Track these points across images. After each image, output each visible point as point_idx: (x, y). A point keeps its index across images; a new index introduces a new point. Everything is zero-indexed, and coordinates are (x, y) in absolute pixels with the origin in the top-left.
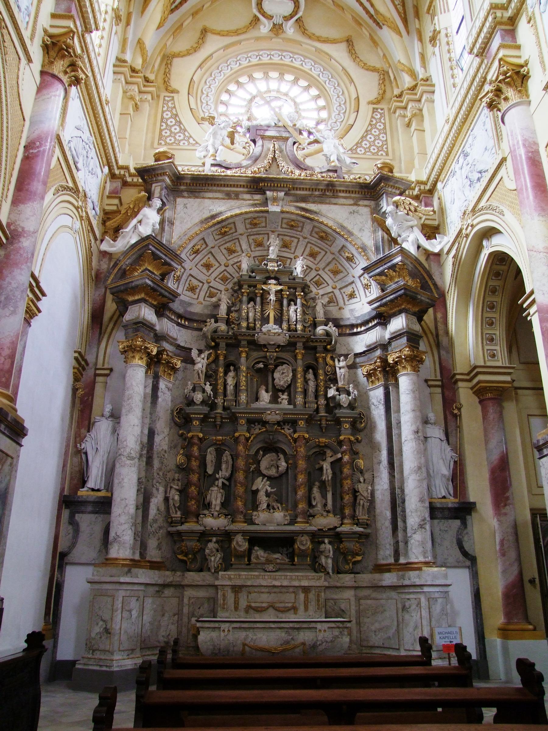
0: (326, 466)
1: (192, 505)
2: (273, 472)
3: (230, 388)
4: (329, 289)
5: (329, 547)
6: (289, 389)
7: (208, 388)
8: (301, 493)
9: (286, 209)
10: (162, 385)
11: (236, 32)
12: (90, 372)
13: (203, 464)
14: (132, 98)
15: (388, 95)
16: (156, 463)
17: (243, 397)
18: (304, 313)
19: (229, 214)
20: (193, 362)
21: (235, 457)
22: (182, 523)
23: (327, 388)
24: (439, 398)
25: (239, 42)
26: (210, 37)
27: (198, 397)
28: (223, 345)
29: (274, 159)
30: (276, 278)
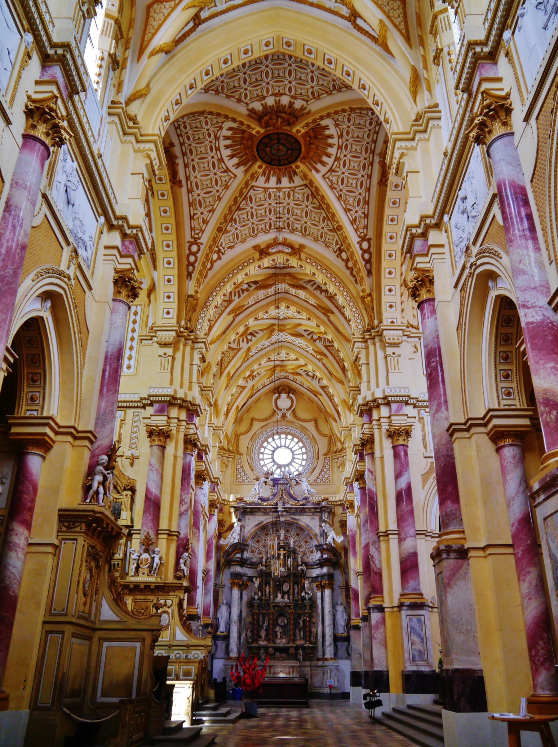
0: (301, 622)
1: (255, 636)
2: (282, 624)
3: (267, 592)
4: (304, 549)
5: (301, 652)
6: (288, 593)
7: (260, 594)
8: (291, 632)
9: (287, 519)
10: (244, 593)
11: (266, 419)
12: (217, 587)
13: (258, 621)
14: (225, 463)
15: (332, 449)
16: (243, 622)
17: (272, 597)
18: (293, 562)
19: (265, 522)
20: (253, 582)
21: (269, 619)
22: (252, 643)
23: (302, 592)
24: (344, 593)
25: (267, 424)
26: (255, 423)
27: (256, 597)
28: (264, 576)
29: (282, 495)
30: (283, 548)
